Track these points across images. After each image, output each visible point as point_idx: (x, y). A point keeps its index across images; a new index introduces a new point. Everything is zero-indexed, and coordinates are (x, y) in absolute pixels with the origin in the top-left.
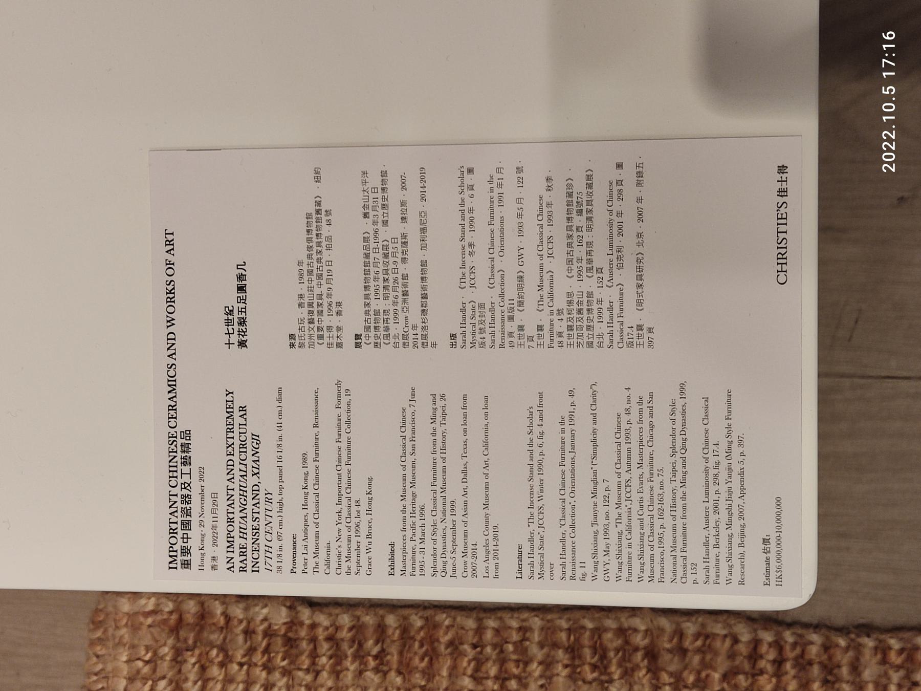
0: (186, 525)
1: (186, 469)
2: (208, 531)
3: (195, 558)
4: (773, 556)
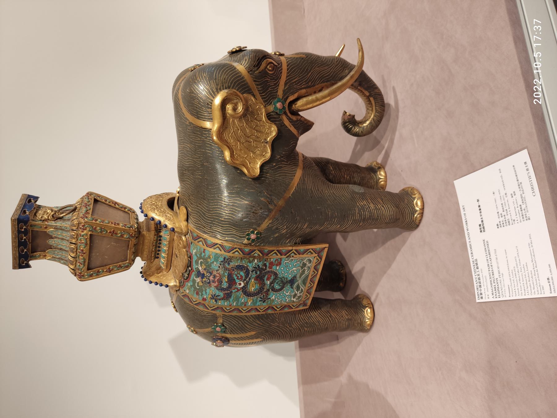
0: (480, 286)
1: (478, 270)
2: (485, 287)
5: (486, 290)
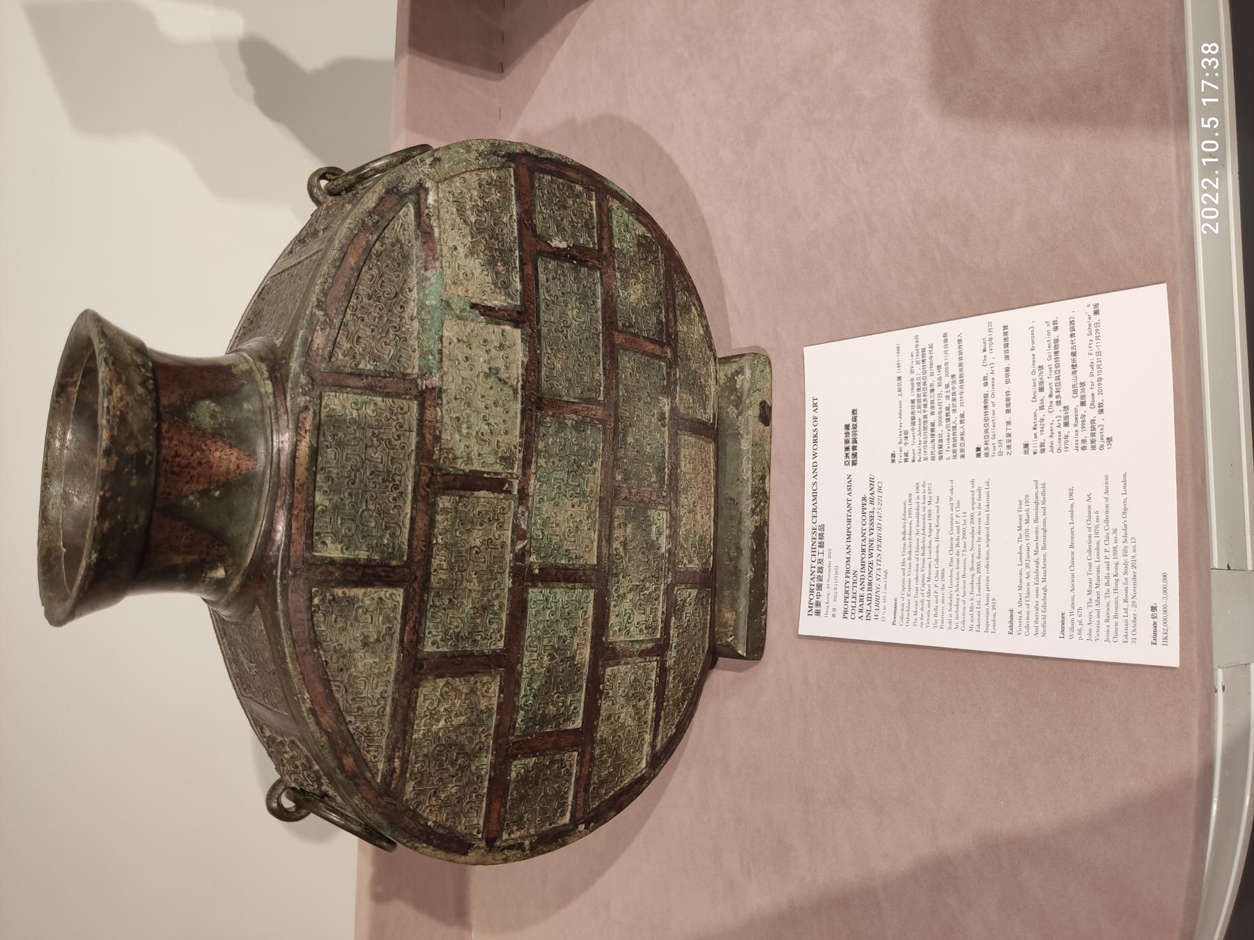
0: (819, 587)
1: (821, 550)
2: (831, 591)
3: (823, 609)
4: (1160, 621)
5: (832, 597)
